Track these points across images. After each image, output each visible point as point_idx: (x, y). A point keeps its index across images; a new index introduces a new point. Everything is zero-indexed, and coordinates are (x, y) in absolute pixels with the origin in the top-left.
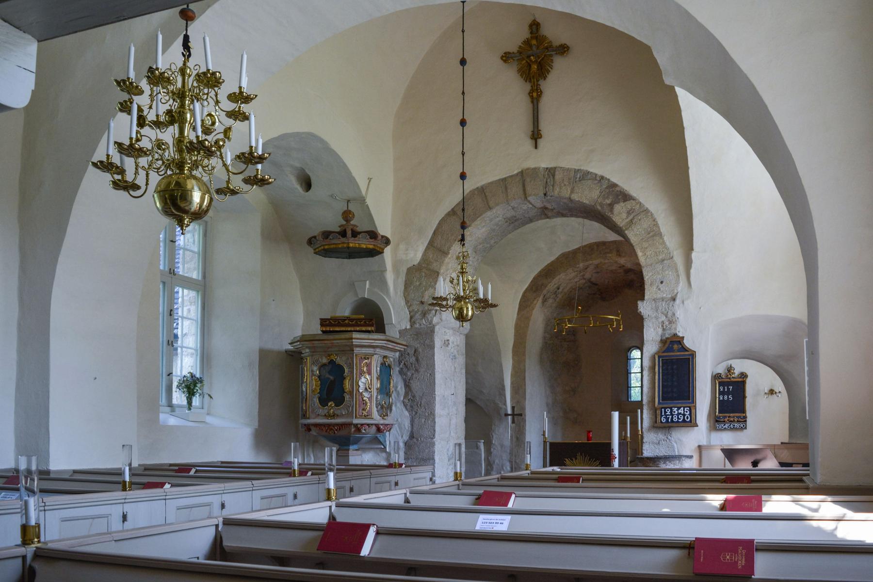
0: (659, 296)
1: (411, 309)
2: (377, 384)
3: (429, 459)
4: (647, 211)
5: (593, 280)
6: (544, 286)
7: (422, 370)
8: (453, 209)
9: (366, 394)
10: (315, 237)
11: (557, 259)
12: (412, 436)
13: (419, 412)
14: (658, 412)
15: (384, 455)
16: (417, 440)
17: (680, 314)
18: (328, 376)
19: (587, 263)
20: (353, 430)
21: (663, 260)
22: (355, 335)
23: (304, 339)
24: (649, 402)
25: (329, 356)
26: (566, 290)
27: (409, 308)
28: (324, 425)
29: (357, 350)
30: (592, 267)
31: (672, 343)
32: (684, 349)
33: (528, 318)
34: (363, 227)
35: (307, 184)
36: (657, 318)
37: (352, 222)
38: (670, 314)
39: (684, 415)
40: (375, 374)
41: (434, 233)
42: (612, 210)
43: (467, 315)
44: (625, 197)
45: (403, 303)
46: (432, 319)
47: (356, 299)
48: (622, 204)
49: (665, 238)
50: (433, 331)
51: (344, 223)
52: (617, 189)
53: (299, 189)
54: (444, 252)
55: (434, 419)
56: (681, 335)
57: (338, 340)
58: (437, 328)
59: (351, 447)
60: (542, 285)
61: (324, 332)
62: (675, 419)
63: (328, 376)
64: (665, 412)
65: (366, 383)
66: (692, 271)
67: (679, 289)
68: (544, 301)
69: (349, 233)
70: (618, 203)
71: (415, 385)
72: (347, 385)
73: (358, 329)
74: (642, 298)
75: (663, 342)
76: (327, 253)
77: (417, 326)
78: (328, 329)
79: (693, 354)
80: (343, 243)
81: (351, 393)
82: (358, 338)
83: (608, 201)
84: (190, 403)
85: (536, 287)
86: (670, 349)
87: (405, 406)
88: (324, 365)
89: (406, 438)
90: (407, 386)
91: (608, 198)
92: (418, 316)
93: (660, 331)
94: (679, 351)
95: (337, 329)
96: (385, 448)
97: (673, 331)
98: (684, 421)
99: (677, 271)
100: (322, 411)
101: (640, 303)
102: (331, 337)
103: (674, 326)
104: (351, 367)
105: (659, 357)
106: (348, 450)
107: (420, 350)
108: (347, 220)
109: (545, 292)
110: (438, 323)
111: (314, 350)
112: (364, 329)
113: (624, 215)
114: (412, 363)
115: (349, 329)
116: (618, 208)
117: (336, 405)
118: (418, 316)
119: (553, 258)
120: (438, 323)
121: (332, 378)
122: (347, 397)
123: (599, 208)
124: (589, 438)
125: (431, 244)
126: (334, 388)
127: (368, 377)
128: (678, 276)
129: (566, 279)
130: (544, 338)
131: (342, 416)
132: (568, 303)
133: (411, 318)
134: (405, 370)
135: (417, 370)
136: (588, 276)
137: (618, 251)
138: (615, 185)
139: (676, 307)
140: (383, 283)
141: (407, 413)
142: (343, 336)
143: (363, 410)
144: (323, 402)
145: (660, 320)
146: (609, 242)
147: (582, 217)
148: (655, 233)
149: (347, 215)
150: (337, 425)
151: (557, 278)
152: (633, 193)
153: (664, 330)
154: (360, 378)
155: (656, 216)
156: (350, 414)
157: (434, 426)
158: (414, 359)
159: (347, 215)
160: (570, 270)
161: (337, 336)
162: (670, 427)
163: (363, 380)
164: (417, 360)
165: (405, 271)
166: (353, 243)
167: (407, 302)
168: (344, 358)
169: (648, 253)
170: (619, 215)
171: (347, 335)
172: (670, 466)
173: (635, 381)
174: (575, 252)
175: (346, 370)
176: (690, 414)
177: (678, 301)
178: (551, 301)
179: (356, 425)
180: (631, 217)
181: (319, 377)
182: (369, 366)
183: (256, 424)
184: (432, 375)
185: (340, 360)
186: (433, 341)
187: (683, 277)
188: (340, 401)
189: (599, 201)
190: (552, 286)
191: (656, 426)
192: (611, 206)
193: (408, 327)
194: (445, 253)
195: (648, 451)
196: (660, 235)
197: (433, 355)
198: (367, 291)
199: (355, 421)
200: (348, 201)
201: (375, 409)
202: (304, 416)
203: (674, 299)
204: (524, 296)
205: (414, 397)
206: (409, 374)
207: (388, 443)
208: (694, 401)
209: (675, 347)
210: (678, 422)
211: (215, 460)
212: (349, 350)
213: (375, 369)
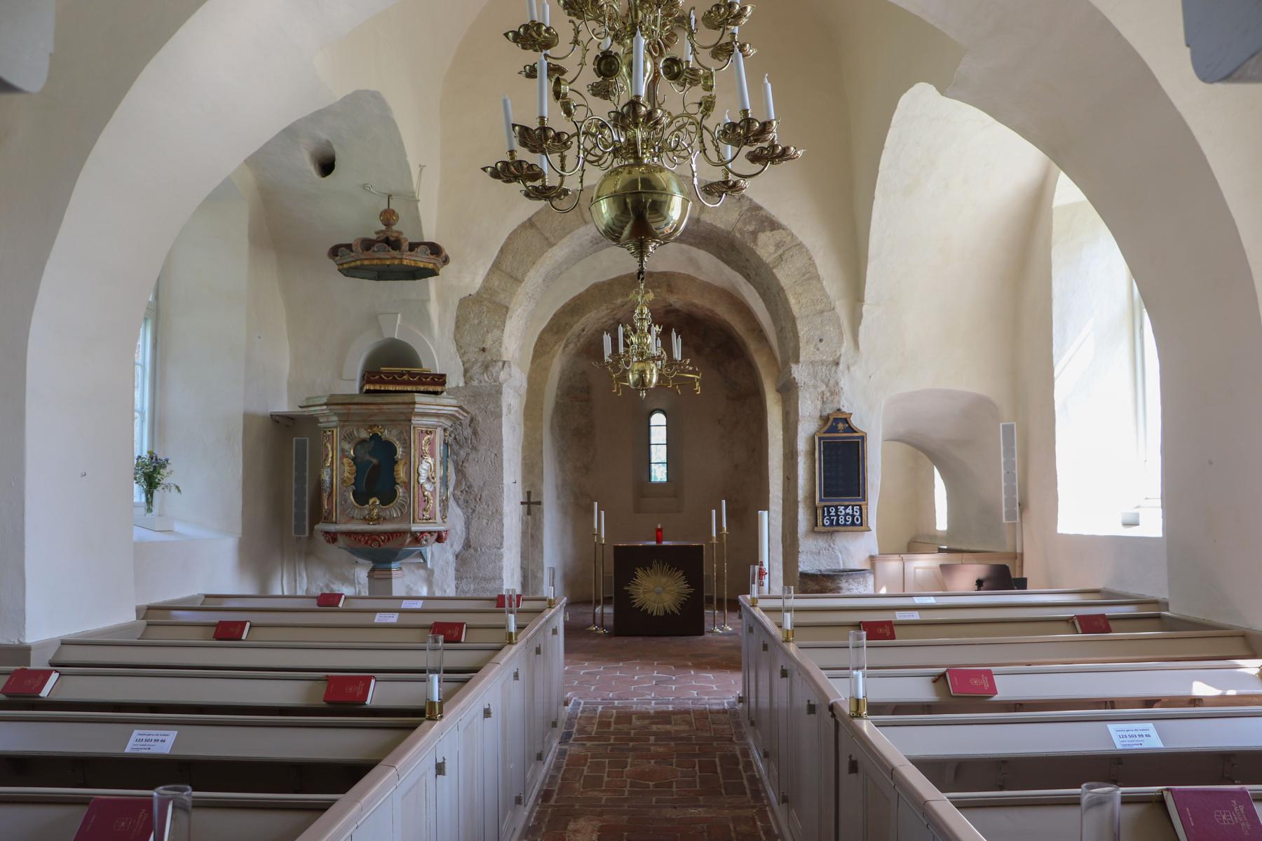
0: (817, 358)
1: (465, 359)
2: (440, 472)
3: (494, 579)
4: (800, 246)
7: (482, 448)
8: (530, 219)
9: (428, 486)
10: (349, 247)
11: (587, 291)
12: (467, 545)
13: (478, 509)
14: (819, 512)
15: (422, 572)
16: (476, 550)
17: (844, 383)
18: (368, 457)
20: (408, 540)
21: (822, 312)
22: (419, 398)
23: (334, 402)
24: (806, 498)
25: (371, 427)
27: (462, 356)
28: (363, 533)
29: (416, 421)
31: (836, 420)
32: (851, 429)
33: (546, 369)
34: (409, 237)
35: (327, 166)
36: (815, 387)
37: (394, 228)
38: (832, 383)
39: (853, 516)
40: (438, 459)
41: (502, 250)
42: (755, 240)
43: (650, 381)
44: (773, 225)
45: (453, 348)
46: (498, 373)
47: (380, 339)
48: (768, 233)
49: (824, 283)
50: (499, 392)
51: (384, 228)
52: (762, 213)
53: (312, 170)
54: (516, 279)
55: (501, 520)
57: (390, 405)
58: (504, 386)
59: (394, 565)
61: (368, 392)
62: (842, 521)
63: (368, 457)
64: (829, 512)
65: (426, 468)
66: (862, 329)
67: (843, 350)
68: (566, 346)
69: (405, 246)
70: (764, 231)
71: (472, 470)
72: (401, 472)
73: (422, 388)
74: (797, 361)
75: (825, 419)
76: (349, 272)
77: (475, 383)
78: (377, 387)
79: (863, 438)
80: (394, 258)
81: (407, 485)
82: (424, 402)
83: (751, 228)
84: (149, 502)
85: (556, 327)
86: (833, 429)
87: (457, 500)
88: (363, 441)
89: (458, 547)
90: (460, 471)
91: (750, 223)
92: (476, 369)
93: (819, 403)
95: (391, 388)
96: (425, 561)
97: (836, 406)
98: (853, 524)
99: (840, 326)
100: (356, 513)
101: (794, 367)
102: (378, 399)
103: (837, 398)
104: (407, 447)
105: (820, 439)
106: (390, 570)
107: (480, 419)
108: (388, 224)
109: (569, 334)
110: (506, 381)
111: (345, 419)
112: (431, 389)
113: (772, 249)
114: (467, 439)
115: (409, 388)
116: (764, 237)
117: (383, 503)
118: (476, 369)
119: (582, 290)
120: (506, 381)
121: (375, 461)
122: (400, 491)
123: (738, 235)
124: (659, 540)
125: (497, 266)
126: (379, 475)
127: (430, 460)
128: (841, 334)
131: (391, 520)
133: (466, 371)
134: (456, 447)
135: (474, 448)
137: (669, 286)
138: (759, 208)
139: (840, 374)
140: (423, 317)
141: (459, 511)
142: (400, 398)
143: (425, 510)
144: (362, 498)
145: (820, 390)
147: (691, 244)
148: (810, 276)
149: (388, 217)
150: (385, 533)
152: (782, 219)
153: (823, 402)
154: (420, 463)
155: (812, 253)
156: (406, 516)
157: (502, 531)
158: (469, 431)
159: (388, 217)
161: (389, 399)
162: (833, 532)
163: (424, 466)
164: (475, 433)
165: (457, 302)
166: (409, 260)
167: (459, 347)
168: (395, 432)
169: (804, 301)
170: (765, 247)
171: (406, 398)
172: (865, 586)
174: (611, 283)
175: (400, 450)
176: (861, 515)
177: (841, 367)
178: (571, 346)
179: (413, 534)
180: (780, 252)
181: (354, 459)
182: (431, 443)
183: (238, 530)
184: (498, 456)
185: (386, 434)
186: (500, 407)
187: (847, 336)
188: (388, 497)
189: (739, 225)
190: (577, 328)
191: (814, 529)
192: (754, 234)
193: (461, 384)
194: (518, 281)
195: (806, 564)
196: (818, 278)
197: (500, 427)
198: (397, 330)
199: (415, 528)
200: (389, 196)
201: (438, 509)
202: (327, 519)
203: (837, 364)
204: (540, 338)
205: (470, 487)
206: (463, 453)
207: (429, 556)
209: (841, 426)
211: (195, 593)
212: (404, 420)
213: (439, 448)
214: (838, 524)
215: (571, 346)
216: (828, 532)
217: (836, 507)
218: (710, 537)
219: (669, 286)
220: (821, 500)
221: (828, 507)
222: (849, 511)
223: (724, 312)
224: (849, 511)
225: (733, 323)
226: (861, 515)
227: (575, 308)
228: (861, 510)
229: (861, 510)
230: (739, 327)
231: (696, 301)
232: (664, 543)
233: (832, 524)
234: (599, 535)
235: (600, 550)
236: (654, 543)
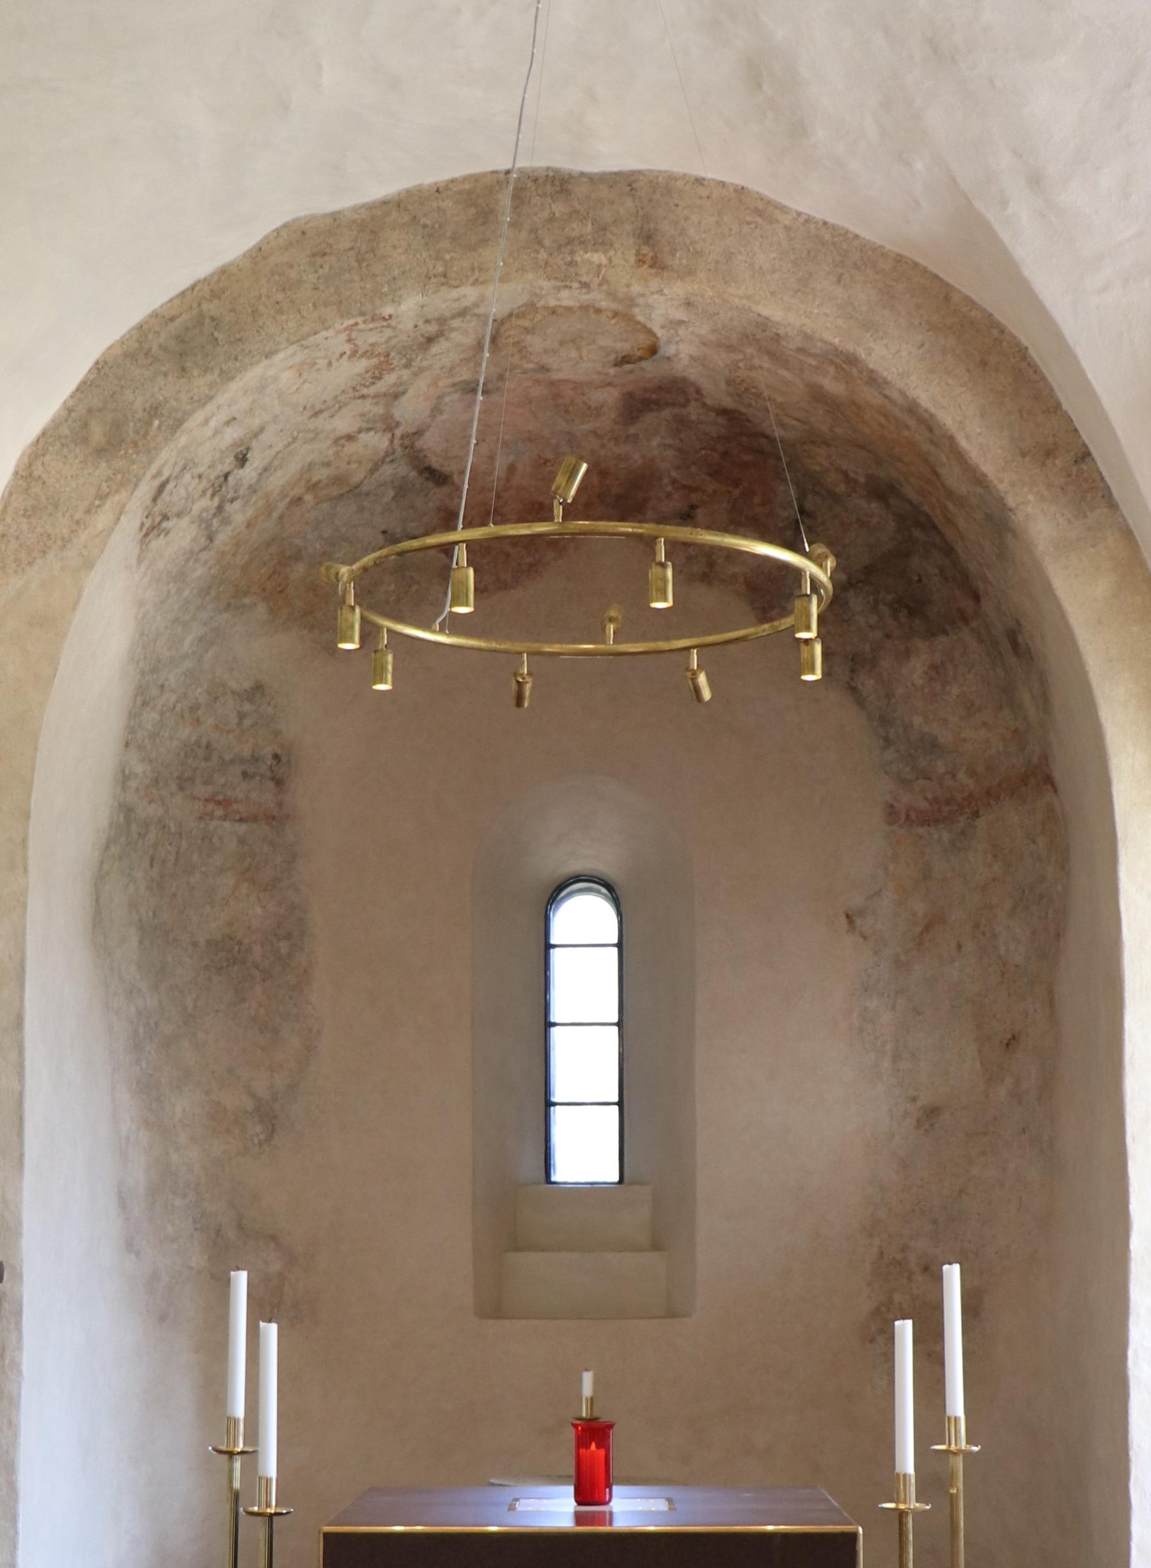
5: (431, 443)
6: (163, 419)
19: (443, 301)
26: (277, 481)
30: (462, 336)
60: (154, 411)
68: (154, 527)
109: (167, 458)
124: (590, 1492)
129: (290, 402)
130: (124, 777)
132: (274, 577)
136: (411, 410)
137: (647, 237)
146: (596, 180)
151: (253, 375)
160: (334, 340)
173: (585, 1063)
174: (372, 224)
215: (183, 534)
218: (891, 1483)
219: (647, 237)
223: (906, 367)
225: (948, 419)
227: (197, 334)
230: (972, 427)
231: (773, 311)
232: (631, 1509)
234: (251, 1456)
235: (253, 1534)
236: (553, 1509)
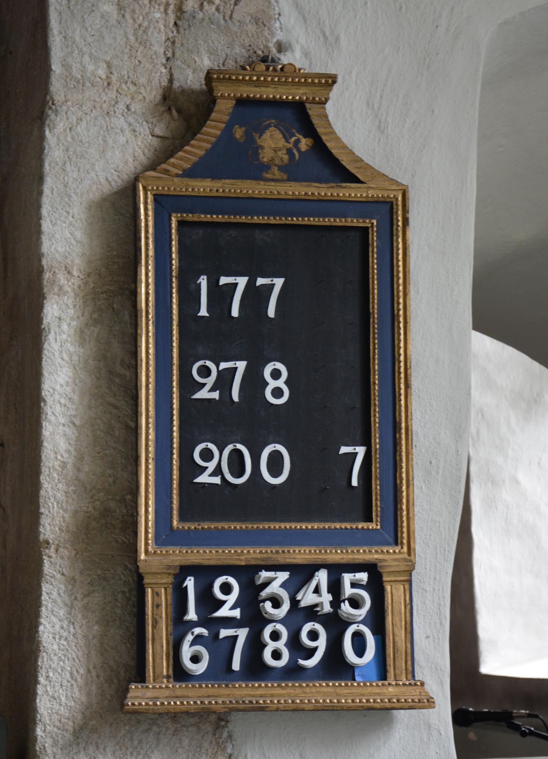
39: (336, 624)
56: (302, 54)
62: (276, 651)
75: (184, 111)
94: (293, 171)
176: (377, 620)
208: (396, 531)
209: (273, 143)
210: (293, 672)
214: (255, 668)
216: (202, 715)
217: (247, 574)
220: (165, 535)
221: (206, 573)
222: (316, 594)
224: (316, 594)
226: (377, 620)
228: (376, 586)
229: (376, 586)
233: (220, 670)
